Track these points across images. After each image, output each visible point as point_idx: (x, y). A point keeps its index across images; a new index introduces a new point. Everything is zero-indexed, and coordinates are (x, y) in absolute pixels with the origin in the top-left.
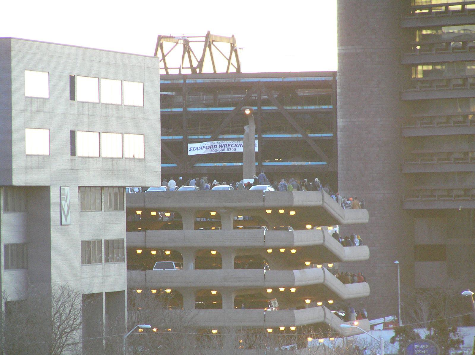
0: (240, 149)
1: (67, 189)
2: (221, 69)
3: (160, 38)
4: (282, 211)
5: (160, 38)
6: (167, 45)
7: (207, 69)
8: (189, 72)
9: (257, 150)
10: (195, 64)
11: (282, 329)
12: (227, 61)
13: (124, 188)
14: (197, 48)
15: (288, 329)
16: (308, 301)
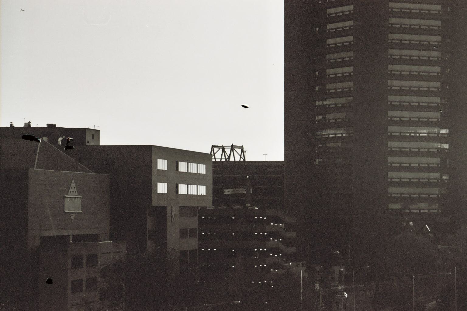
0: (245, 192)
1: (174, 208)
2: (237, 159)
3: (213, 146)
4: (261, 217)
5: (213, 146)
6: (216, 150)
7: (232, 159)
8: (224, 160)
9: (251, 192)
10: (227, 157)
11: (261, 265)
12: (240, 156)
13: (197, 207)
14: (228, 151)
15: (263, 266)
16: (271, 254)
